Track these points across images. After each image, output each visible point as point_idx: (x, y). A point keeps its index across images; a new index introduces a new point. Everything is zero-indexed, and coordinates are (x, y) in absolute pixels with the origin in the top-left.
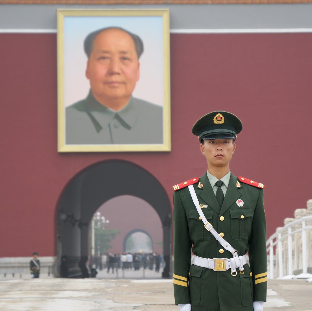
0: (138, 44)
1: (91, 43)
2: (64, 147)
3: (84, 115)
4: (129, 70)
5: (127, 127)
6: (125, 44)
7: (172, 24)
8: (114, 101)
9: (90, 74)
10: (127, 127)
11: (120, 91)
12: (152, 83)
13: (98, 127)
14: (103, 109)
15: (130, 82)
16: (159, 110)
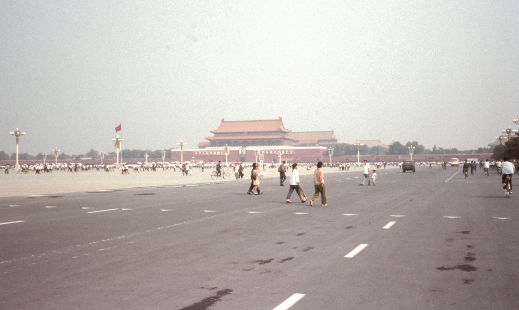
12: (244, 153)
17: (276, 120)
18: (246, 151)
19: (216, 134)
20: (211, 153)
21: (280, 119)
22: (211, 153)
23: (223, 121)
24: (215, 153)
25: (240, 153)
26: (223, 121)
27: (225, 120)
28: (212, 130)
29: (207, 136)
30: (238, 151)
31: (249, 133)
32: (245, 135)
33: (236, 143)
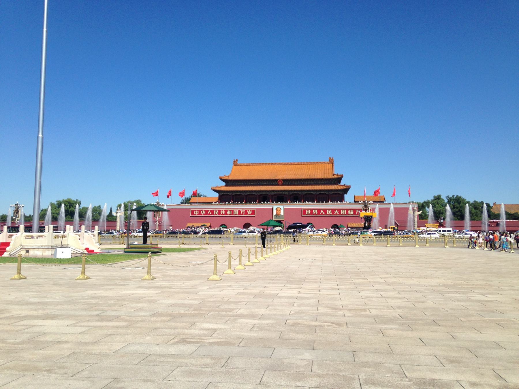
6: (279, 209)
12: (282, 213)
17: (324, 163)
18: (284, 209)
19: (228, 182)
20: (223, 212)
21: (331, 161)
22: (223, 212)
23: (235, 163)
24: (229, 213)
25: (275, 213)
27: (238, 163)
28: (222, 175)
29: (214, 186)
31: (286, 182)
32: (278, 185)
33: (264, 198)
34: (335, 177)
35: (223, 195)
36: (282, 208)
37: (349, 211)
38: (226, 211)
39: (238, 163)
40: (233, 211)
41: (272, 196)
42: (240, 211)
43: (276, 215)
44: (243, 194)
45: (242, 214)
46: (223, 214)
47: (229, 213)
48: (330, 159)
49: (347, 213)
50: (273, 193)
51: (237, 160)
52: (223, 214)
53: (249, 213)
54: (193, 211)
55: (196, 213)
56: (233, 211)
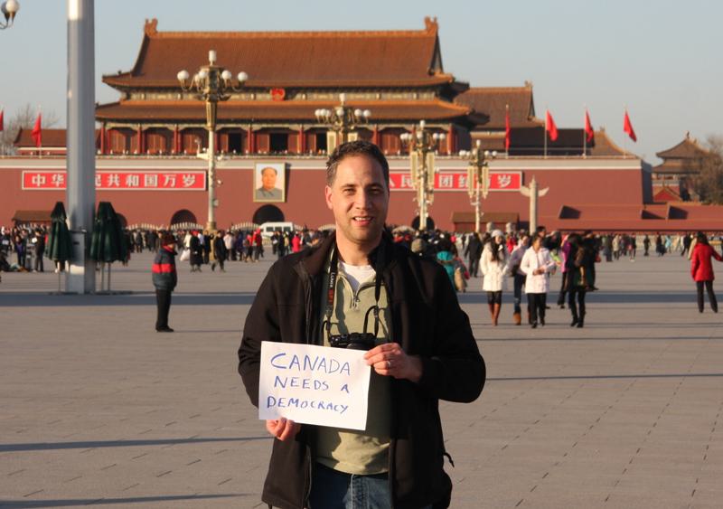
0: (276, 172)
1: (263, 172)
2: (255, 201)
3: (261, 193)
4: (272, 179)
5: (272, 195)
6: (273, 172)
7: (287, 165)
8: (269, 188)
9: (263, 180)
10: (272, 195)
11: (271, 185)
12: (280, 183)
13: (264, 195)
14: (266, 190)
15: (274, 182)
16: (279, 191)
18: (288, 172)
21: (432, 25)
22: (114, 180)
23: (150, 26)
24: (132, 181)
25: (258, 184)
26: (150, 26)
30: (249, 174)
34: (432, 81)
35: (113, 129)
36: (280, 168)
37: (461, 179)
38: (123, 177)
39: (160, 28)
40: (141, 177)
41: (256, 133)
42: (161, 178)
43: (263, 189)
44: (172, 127)
45: (168, 186)
46: (114, 185)
47: (132, 181)
48: (427, 20)
49: (456, 184)
50: (256, 127)
51: (155, 22)
52: (114, 185)
53: (189, 182)
54: (28, 177)
55: (39, 181)
56: (141, 177)
